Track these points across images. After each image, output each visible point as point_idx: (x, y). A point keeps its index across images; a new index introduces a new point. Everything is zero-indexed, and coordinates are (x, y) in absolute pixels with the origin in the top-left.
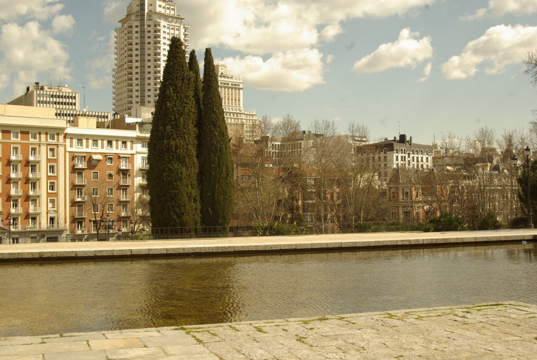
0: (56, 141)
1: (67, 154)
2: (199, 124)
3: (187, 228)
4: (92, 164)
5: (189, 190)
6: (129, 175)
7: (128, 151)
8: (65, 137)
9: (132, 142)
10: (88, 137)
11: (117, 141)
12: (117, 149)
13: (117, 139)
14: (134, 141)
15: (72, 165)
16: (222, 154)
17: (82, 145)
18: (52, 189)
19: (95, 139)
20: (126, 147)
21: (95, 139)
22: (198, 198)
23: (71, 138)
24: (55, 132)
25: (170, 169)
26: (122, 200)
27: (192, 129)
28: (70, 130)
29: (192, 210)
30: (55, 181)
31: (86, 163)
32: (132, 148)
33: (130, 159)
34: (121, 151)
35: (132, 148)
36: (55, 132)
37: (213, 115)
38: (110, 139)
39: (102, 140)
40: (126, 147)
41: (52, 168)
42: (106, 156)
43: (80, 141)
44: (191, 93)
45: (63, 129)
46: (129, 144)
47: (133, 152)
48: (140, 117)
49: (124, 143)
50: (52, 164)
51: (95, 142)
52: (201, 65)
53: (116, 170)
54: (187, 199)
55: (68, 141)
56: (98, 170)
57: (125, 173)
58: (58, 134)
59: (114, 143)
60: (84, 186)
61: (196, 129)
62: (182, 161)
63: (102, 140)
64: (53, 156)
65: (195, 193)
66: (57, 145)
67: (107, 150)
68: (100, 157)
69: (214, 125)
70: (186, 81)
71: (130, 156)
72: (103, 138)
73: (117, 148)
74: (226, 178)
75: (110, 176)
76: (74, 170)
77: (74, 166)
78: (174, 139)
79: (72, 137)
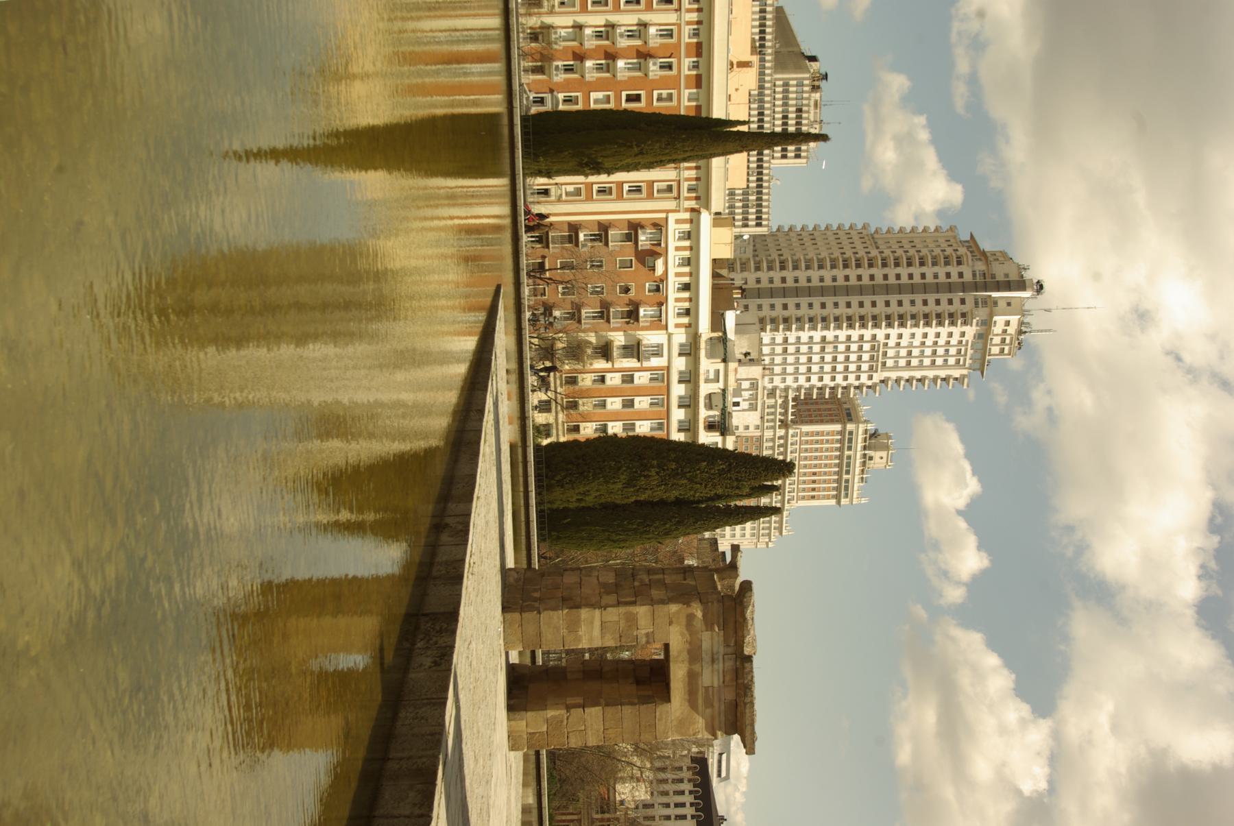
0: (686, 195)
1: (663, 215)
2: (679, 502)
3: (545, 493)
4: (647, 257)
5: (594, 493)
6: (628, 323)
7: (672, 320)
8: (693, 210)
9: (689, 326)
10: (695, 249)
11: (690, 300)
12: (674, 299)
13: (694, 300)
14: (691, 330)
15: (643, 223)
16: (641, 533)
17: (680, 239)
18: (599, 191)
19: (692, 262)
20: (679, 315)
21: (691, 262)
22: (583, 504)
23: (691, 221)
24: (701, 193)
25: (619, 469)
26: (583, 311)
27: (673, 494)
28: (706, 218)
29: (567, 498)
30: (614, 196)
31: (648, 247)
32: (677, 326)
33: (659, 323)
34: (672, 307)
35: (677, 326)
36: (701, 193)
37: (692, 520)
38: (692, 287)
39: (691, 274)
40: (679, 315)
41: (638, 190)
42: (662, 281)
43: (688, 236)
44: (720, 491)
45: (708, 207)
46: (685, 320)
47: (671, 328)
48: (737, 332)
49: (687, 312)
50: (644, 190)
51: (687, 262)
52: (764, 501)
53: (636, 299)
54: (582, 490)
55: (687, 216)
56: (637, 269)
57: (632, 315)
58: (697, 198)
59: (686, 295)
60: (607, 244)
61: (672, 498)
62: (628, 484)
63: (691, 274)
64: (658, 191)
65: (590, 500)
66: (678, 198)
67: (673, 283)
68: (660, 270)
69: (678, 522)
70: (735, 484)
71: (664, 322)
72: (695, 274)
73: (677, 300)
74: (609, 539)
75: (626, 290)
76: (634, 228)
77: (642, 227)
78: (658, 473)
79: (695, 221)
